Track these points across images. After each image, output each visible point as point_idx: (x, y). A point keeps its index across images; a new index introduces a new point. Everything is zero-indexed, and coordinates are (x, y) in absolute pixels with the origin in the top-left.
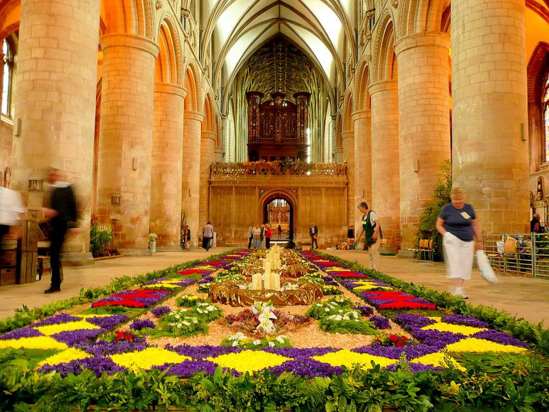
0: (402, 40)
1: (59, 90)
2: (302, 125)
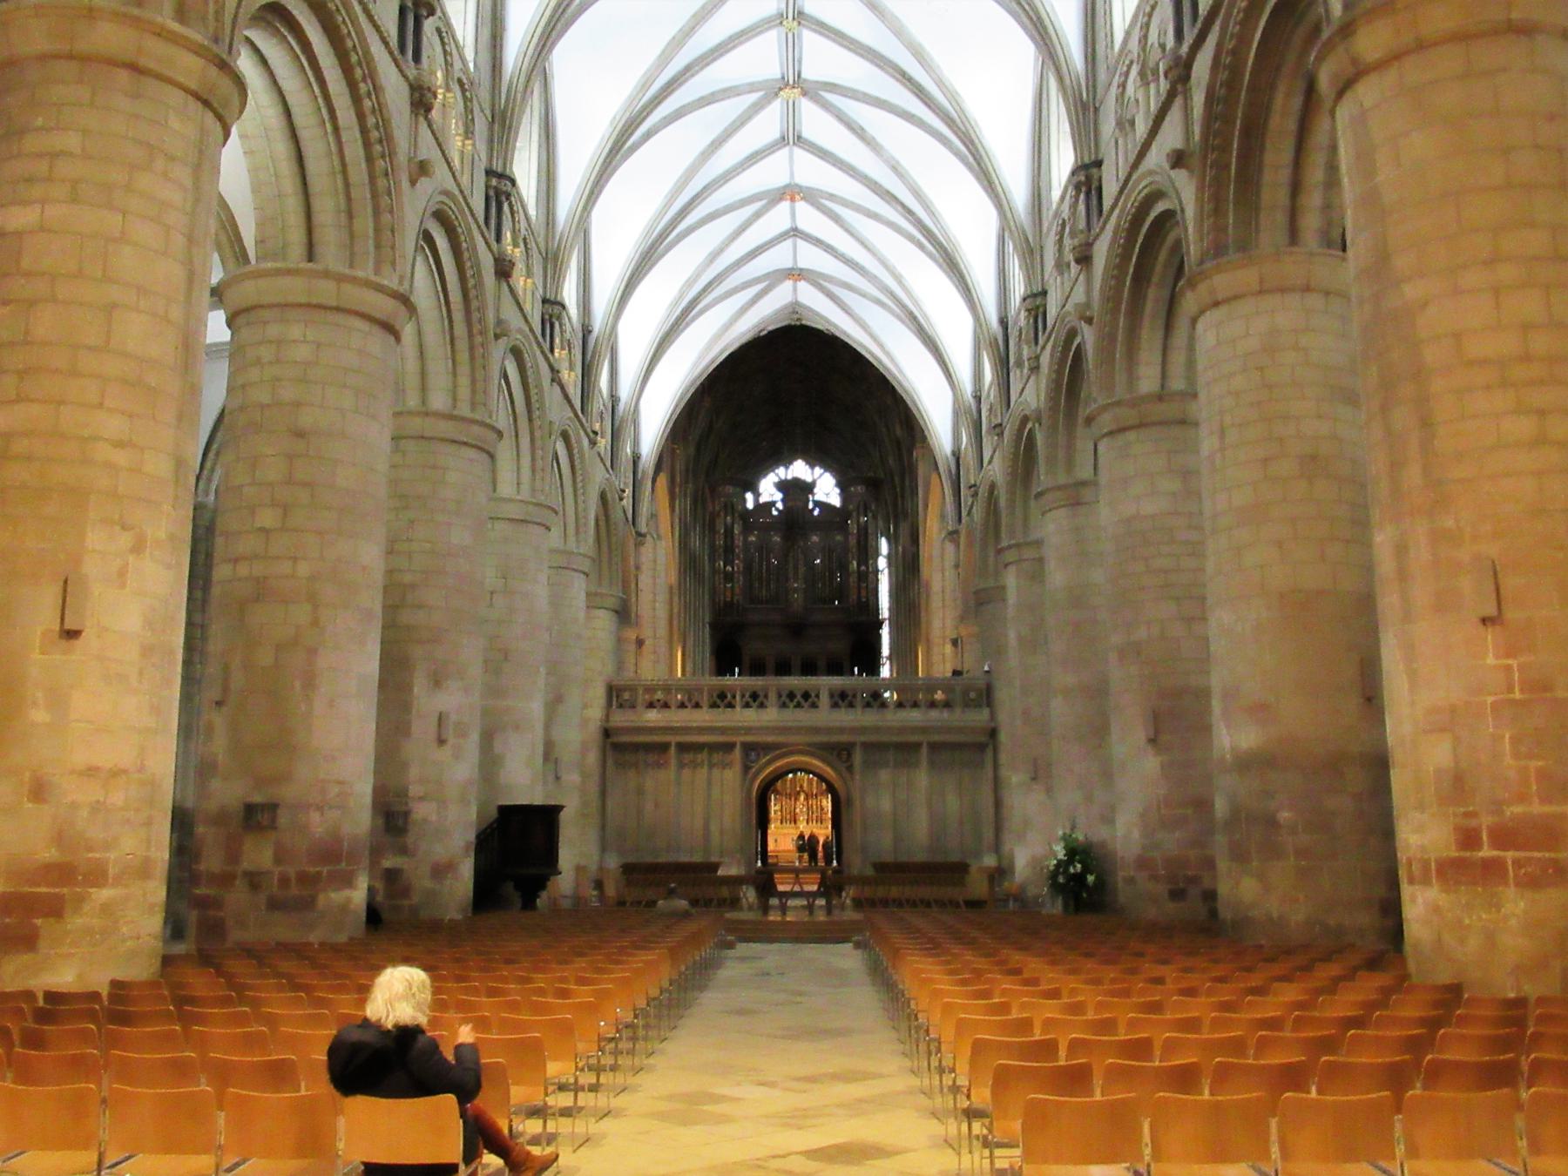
0: (1105, 408)
1: (312, 598)
2: (863, 568)
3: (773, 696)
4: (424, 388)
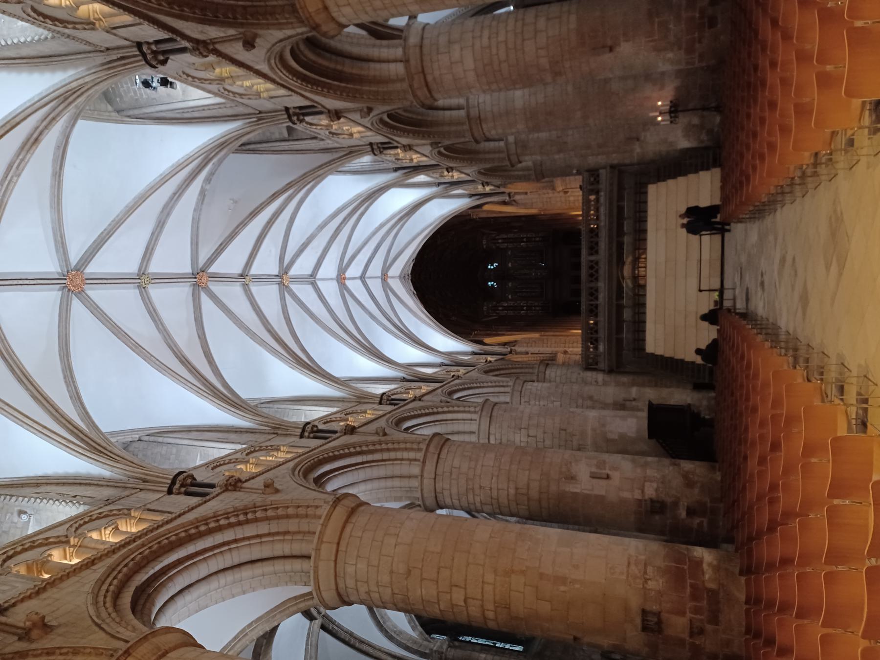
3: (592, 285)
4: (410, 477)
